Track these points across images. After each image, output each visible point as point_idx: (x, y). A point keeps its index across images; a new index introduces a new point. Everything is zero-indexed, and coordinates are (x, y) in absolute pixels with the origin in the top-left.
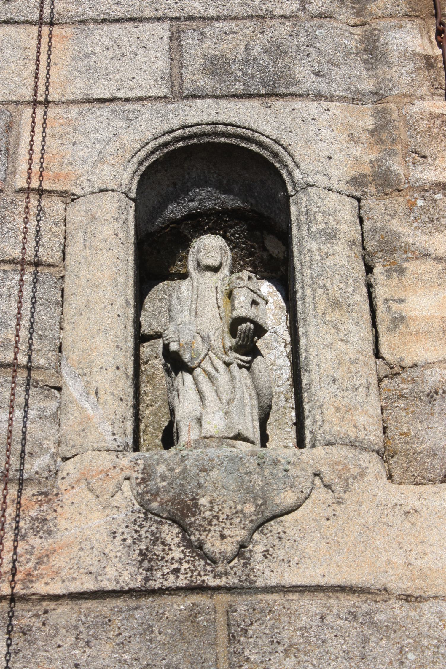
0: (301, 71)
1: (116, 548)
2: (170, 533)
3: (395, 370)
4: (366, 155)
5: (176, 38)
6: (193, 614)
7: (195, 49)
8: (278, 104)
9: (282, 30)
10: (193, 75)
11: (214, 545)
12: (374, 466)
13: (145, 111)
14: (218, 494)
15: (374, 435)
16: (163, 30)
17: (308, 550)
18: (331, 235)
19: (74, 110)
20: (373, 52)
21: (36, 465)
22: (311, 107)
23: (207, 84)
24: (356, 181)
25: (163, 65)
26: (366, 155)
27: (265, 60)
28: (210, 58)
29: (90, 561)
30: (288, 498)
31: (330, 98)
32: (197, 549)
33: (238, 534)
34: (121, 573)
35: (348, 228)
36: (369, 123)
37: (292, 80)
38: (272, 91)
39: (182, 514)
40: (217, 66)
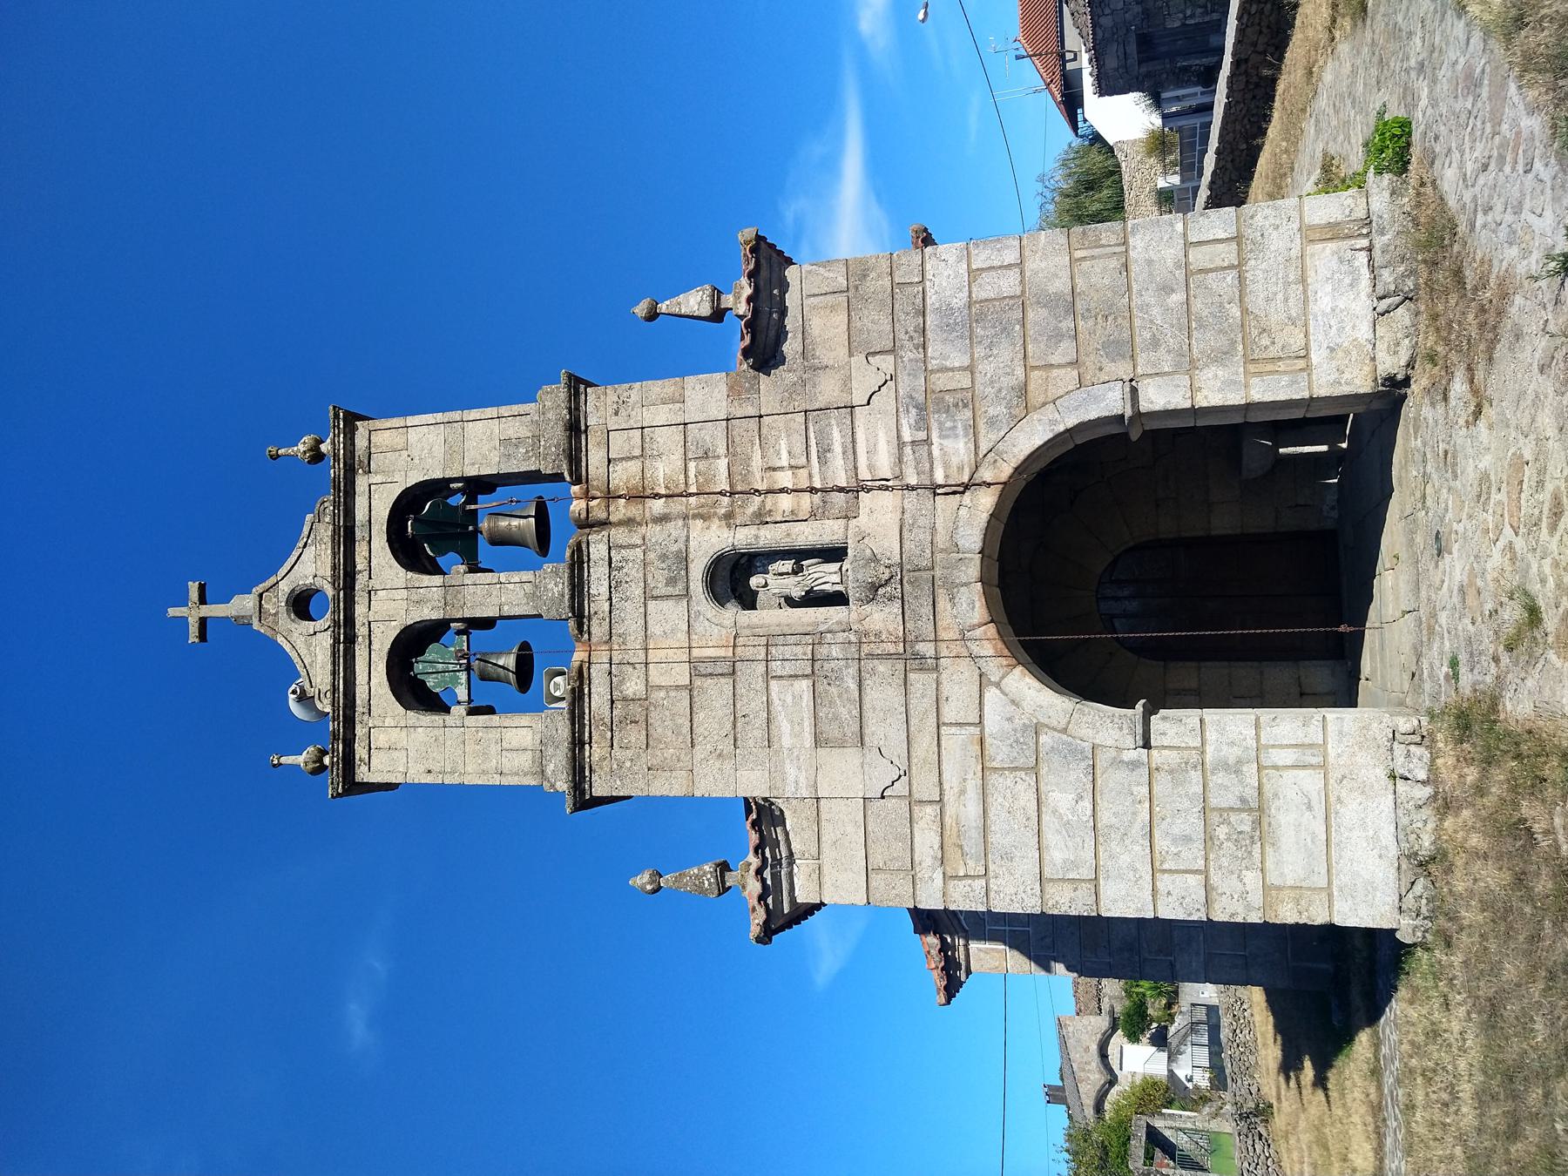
0: (674, 548)
1: (887, 610)
2: (881, 591)
3: (813, 515)
4: (715, 523)
5: (655, 598)
6: (910, 582)
7: (662, 590)
8: (691, 556)
9: (652, 556)
10: (679, 589)
11: (886, 576)
12: (853, 522)
13: (695, 608)
14: (868, 575)
15: (842, 522)
16: (651, 604)
17: (888, 546)
18: (757, 537)
19: (693, 636)
20: (663, 519)
21: (853, 638)
22: (692, 543)
23: (680, 587)
24: (729, 526)
25: (671, 603)
26: (715, 523)
27: (669, 562)
28: (667, 585)
29: (892, 617)
30: (868, 552)
31: (688, 537)
32: (887, 581)
33: (882, 569)
34: (896, 607)
35: (753, 530)
36: (699, 522)
37: (680, 551)
38: (684, 559)
39: (875, 588)
40: (671, 581)
